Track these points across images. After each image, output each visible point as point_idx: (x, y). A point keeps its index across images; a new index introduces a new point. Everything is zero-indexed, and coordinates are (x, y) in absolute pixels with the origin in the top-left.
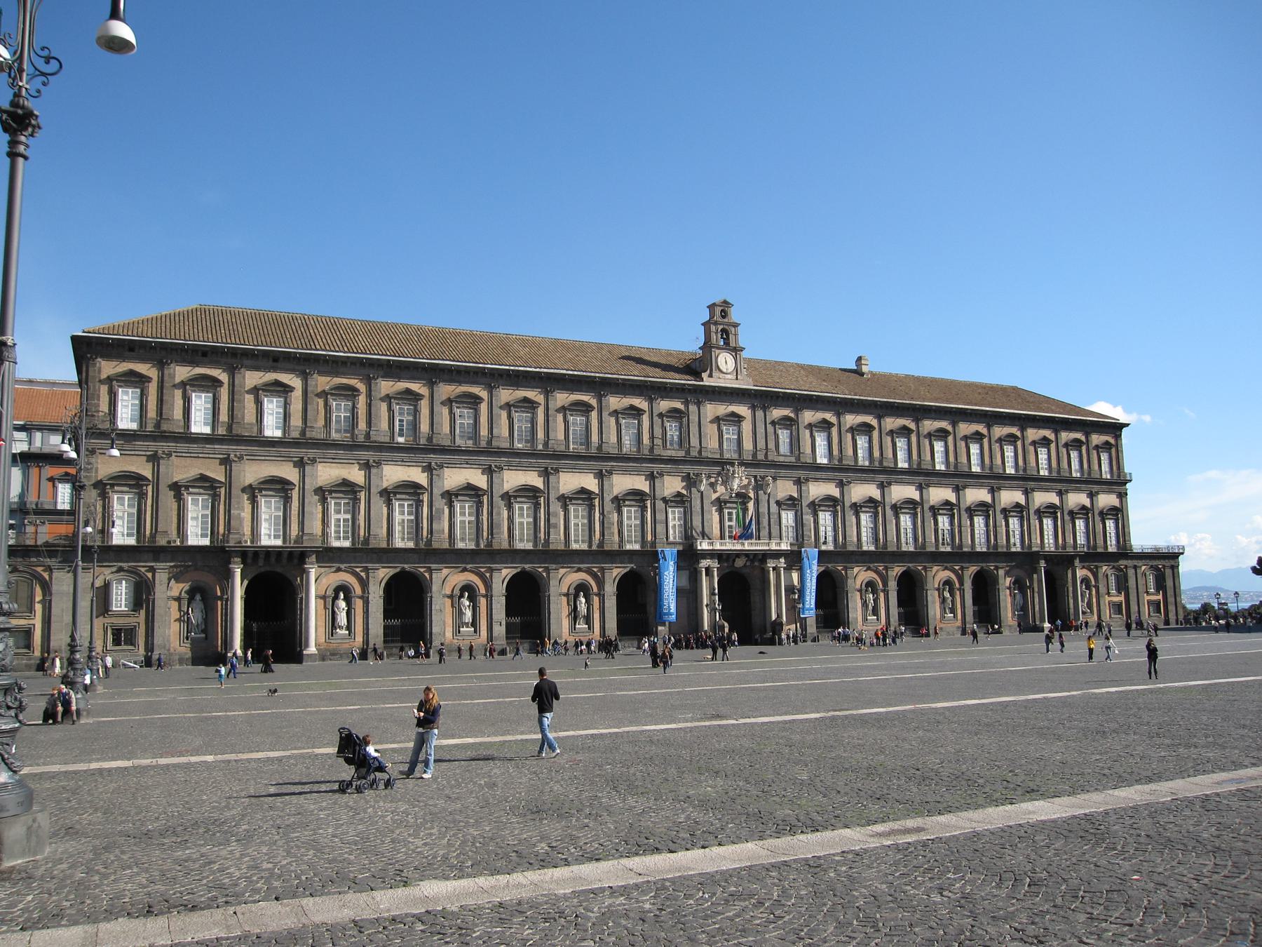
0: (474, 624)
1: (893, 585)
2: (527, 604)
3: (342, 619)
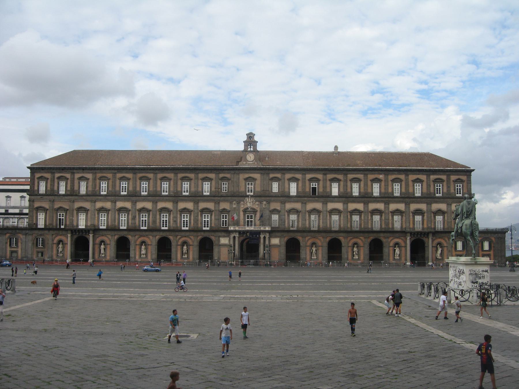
0: (146, 254)
1: (326, 245)
2: (123, 247)
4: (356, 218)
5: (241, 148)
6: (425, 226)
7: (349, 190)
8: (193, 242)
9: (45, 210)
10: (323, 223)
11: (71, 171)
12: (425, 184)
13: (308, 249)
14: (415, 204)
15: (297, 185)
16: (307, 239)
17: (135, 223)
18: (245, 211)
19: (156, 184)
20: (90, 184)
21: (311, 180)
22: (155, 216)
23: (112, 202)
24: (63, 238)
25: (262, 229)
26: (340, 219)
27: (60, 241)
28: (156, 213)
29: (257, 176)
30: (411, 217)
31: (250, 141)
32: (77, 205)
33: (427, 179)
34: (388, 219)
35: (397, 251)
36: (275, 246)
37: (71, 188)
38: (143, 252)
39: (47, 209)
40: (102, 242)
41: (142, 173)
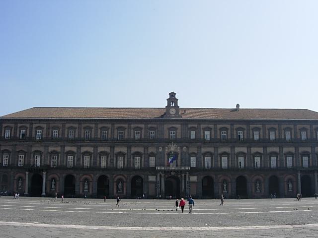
0: (88, 189)
3: (53, 186)
4: (257, 159)
5: (164, 104)
6: (311, 165)
7: (251, 137)
8: (127, 179)
9: (8, 152)
10: (231, 163)
11: (31, 122)
12: (309, 131)
13: (220, 185)
14: (302, 148)
15: (210, 133)
16: (219, 176)
17: (80, 164)
18: (169, 154)
19: (97, 132)
20: (45, 132)
21: (221, 129)
22: (95, 159)
23: (61, 146)
24: (22, 175)
25: (183, 168)
26: (245, 161)
27: (20, 177)
28: (97, 156)
29: (178, 126)
30: (300, 158)
31: (172, 98)
32: (34, 149)
33: (310, 128)
34: (283, 160)
35: (290, 185)
36: (193, 182)
37: (29, 135)
38: (86, 187)
39: (10, 152)
40: (53, 178)
41: (86, 124)
